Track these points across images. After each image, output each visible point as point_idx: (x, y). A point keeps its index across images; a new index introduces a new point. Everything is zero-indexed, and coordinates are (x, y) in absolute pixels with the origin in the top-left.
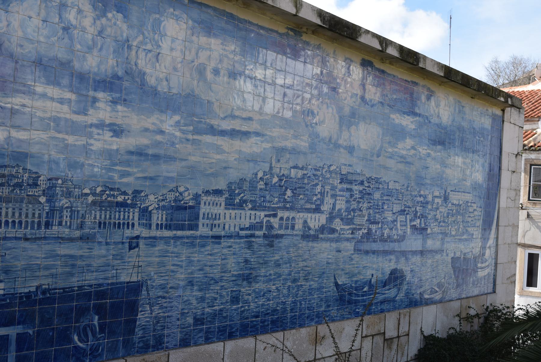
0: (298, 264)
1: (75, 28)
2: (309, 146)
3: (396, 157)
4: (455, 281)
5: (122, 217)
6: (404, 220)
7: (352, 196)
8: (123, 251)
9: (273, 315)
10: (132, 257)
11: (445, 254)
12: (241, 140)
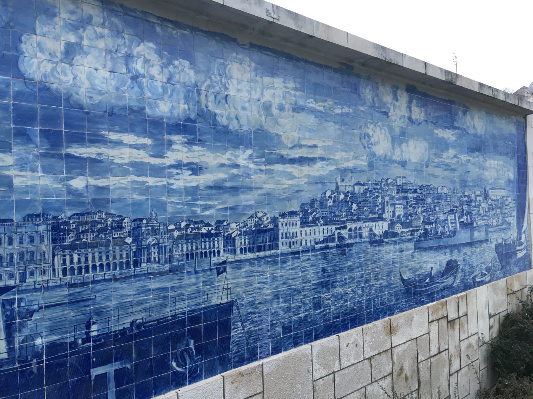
0: (368, 267)
1: (143, 76)
2: (368, 164)
3: (442, 166)
4: (500, 264)
5: (208, 246)
6: (453, 218)
7: (408, 203)
8: (212, 277)
9: (352, 314)
10: (221, 281)
11: (489, 243)
12: (308, 165)
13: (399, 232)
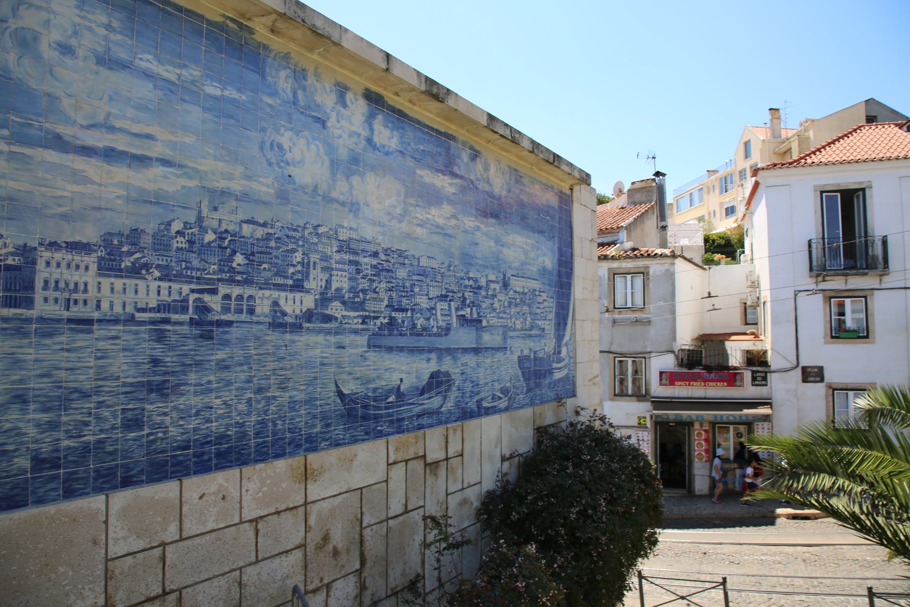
6: (447, 308)
7: (358, 271)
13: (339, 316)
